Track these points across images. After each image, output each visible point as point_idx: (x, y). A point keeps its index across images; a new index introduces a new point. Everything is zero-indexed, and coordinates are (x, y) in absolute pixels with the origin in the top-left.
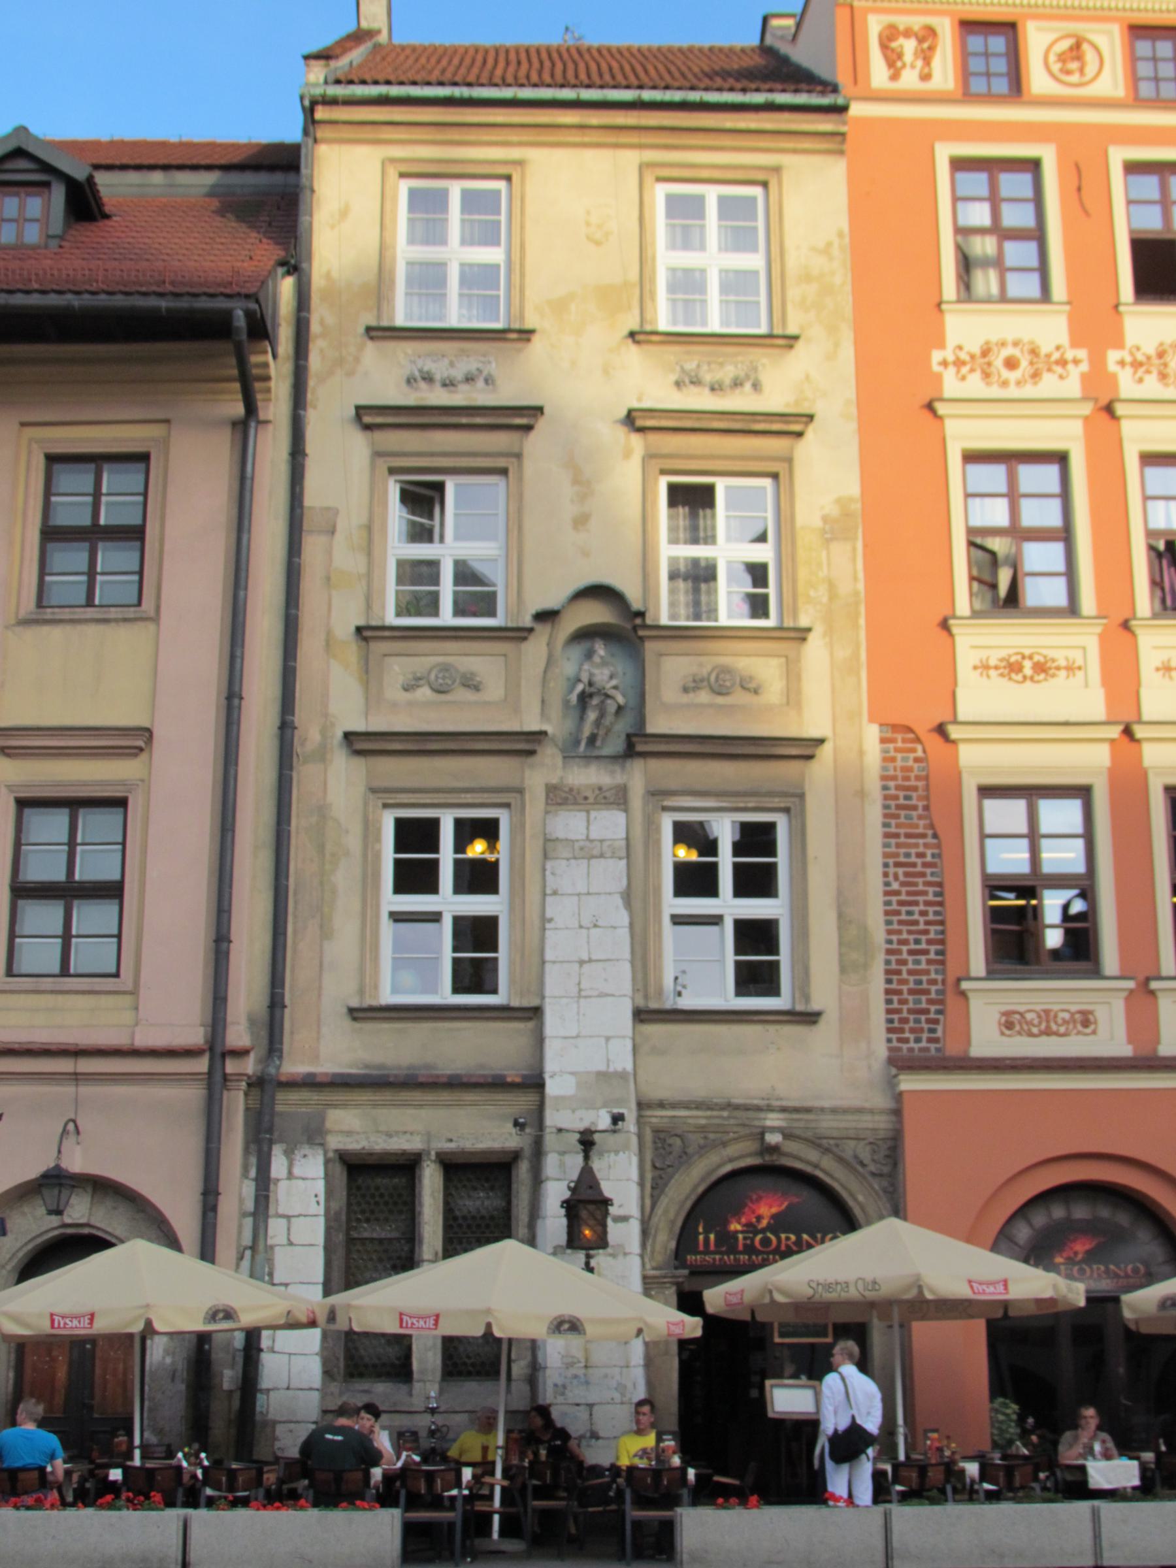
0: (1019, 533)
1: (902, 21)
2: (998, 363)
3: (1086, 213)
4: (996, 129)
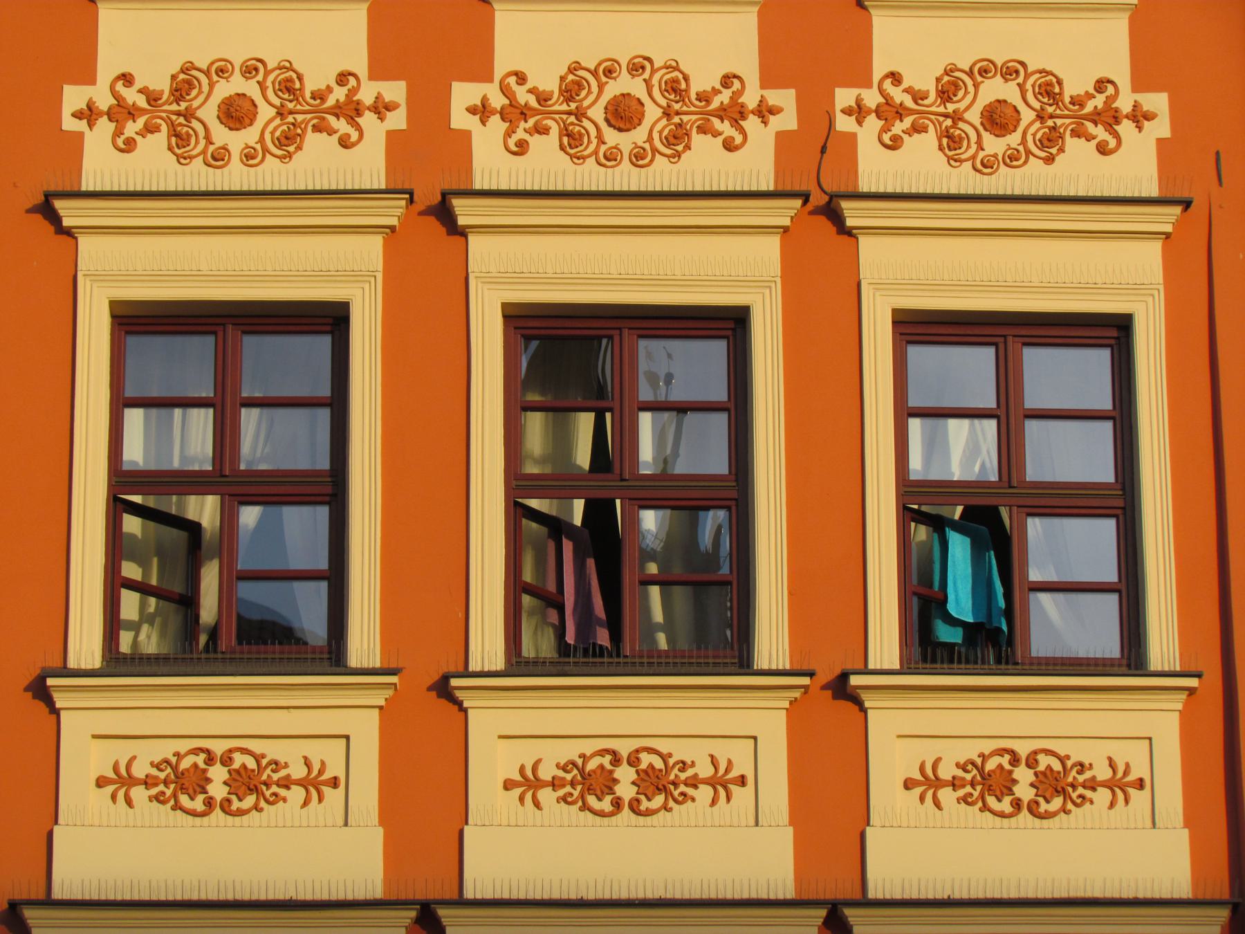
0: (231, 481)
2: (209, 112)
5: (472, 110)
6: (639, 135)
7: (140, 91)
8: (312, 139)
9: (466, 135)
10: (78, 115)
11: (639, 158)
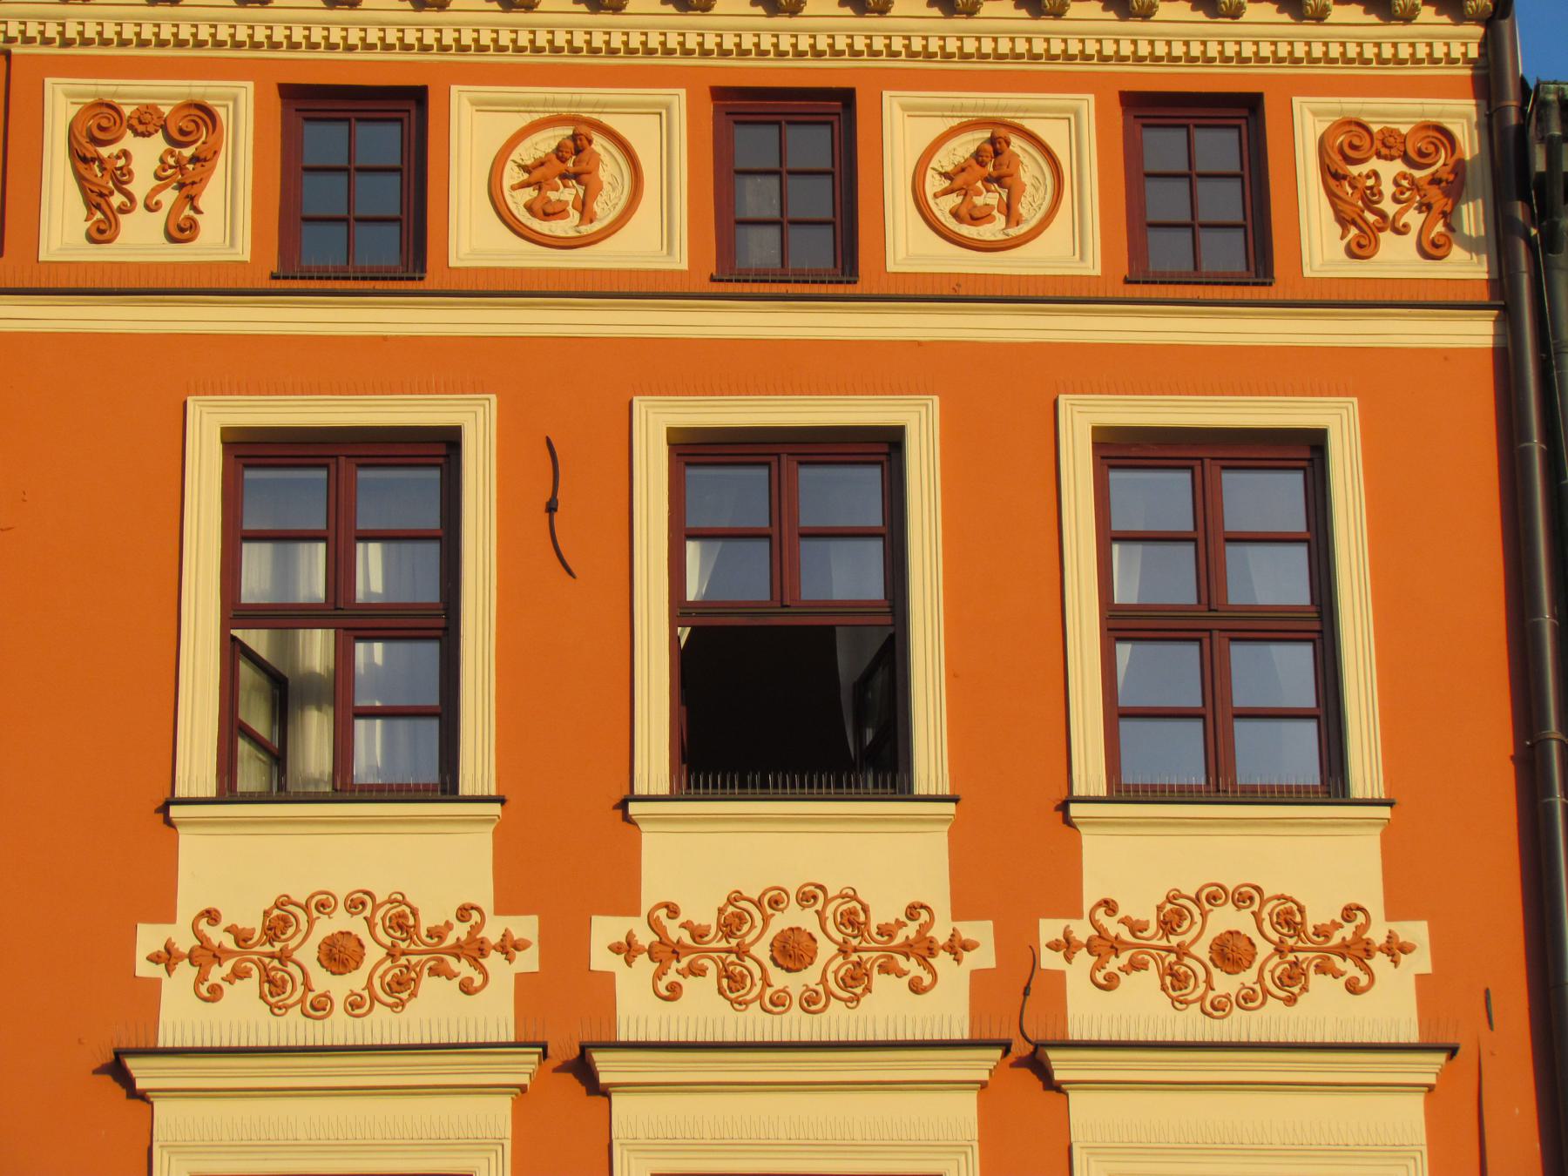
1: (131, 93)
2: (308, 954)
3: (570, 572)
4: (349, 361)
5: (616, 949)
6: (811, 976)
7: (227, 930)
8: (428, 984)
9: (608, 978)
10: (154, 959)
11: (810, 1002)
